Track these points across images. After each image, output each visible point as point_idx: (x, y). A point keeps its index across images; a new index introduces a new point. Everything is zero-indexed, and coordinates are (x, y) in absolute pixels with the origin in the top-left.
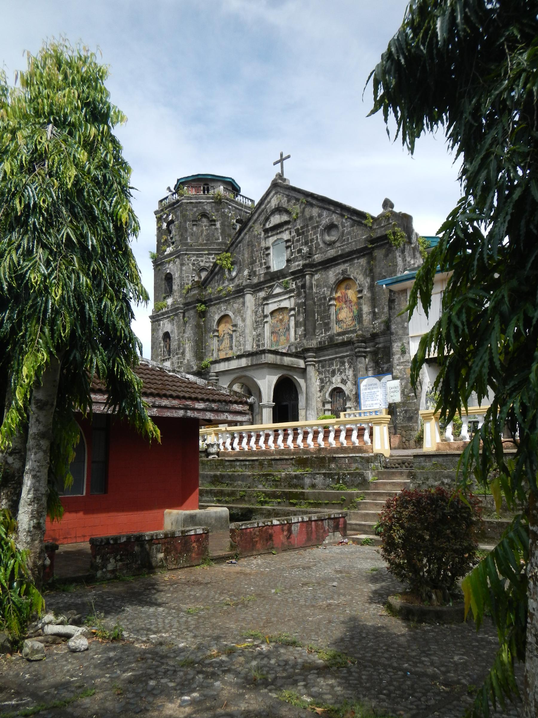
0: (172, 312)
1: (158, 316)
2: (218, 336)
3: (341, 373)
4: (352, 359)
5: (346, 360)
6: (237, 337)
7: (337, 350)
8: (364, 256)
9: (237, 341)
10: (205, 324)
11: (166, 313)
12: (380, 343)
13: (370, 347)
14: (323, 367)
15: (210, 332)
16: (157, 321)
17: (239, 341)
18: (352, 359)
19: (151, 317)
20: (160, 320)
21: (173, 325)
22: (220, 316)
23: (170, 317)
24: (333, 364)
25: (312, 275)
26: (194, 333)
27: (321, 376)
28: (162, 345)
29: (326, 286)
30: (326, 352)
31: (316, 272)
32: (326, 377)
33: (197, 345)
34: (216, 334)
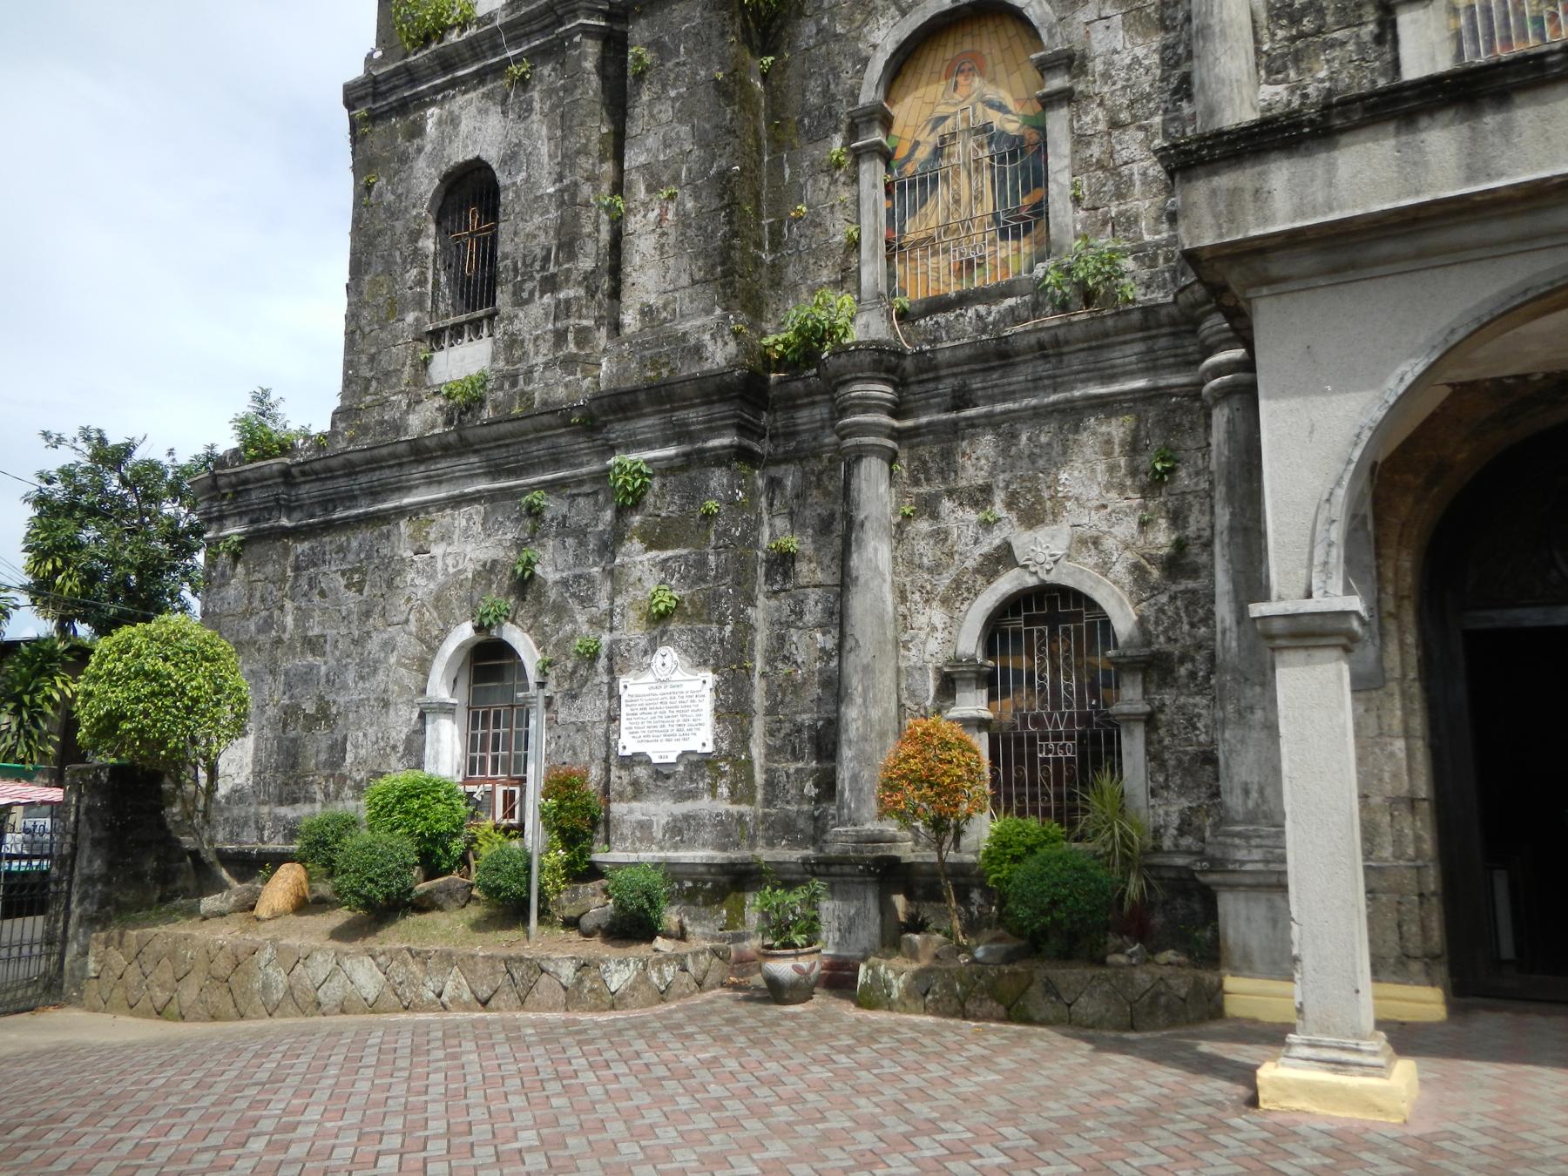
0: (514, 41)
1: (411, 75)
2: (887, 157)
6: (1080, 140)
9: (1081, 166)
10: (773, 93)
11: (474, 48)
15: (818, 135)
16: (402, 108)
17: (1106, 166)
19: (353, 96)
20: (421, 102)
21: (526, 112)
22: (916, 20)
23: (499, 70)
26: (701, 140)
28: (429, 244)
33: (731, 207)
34: (878, 136)
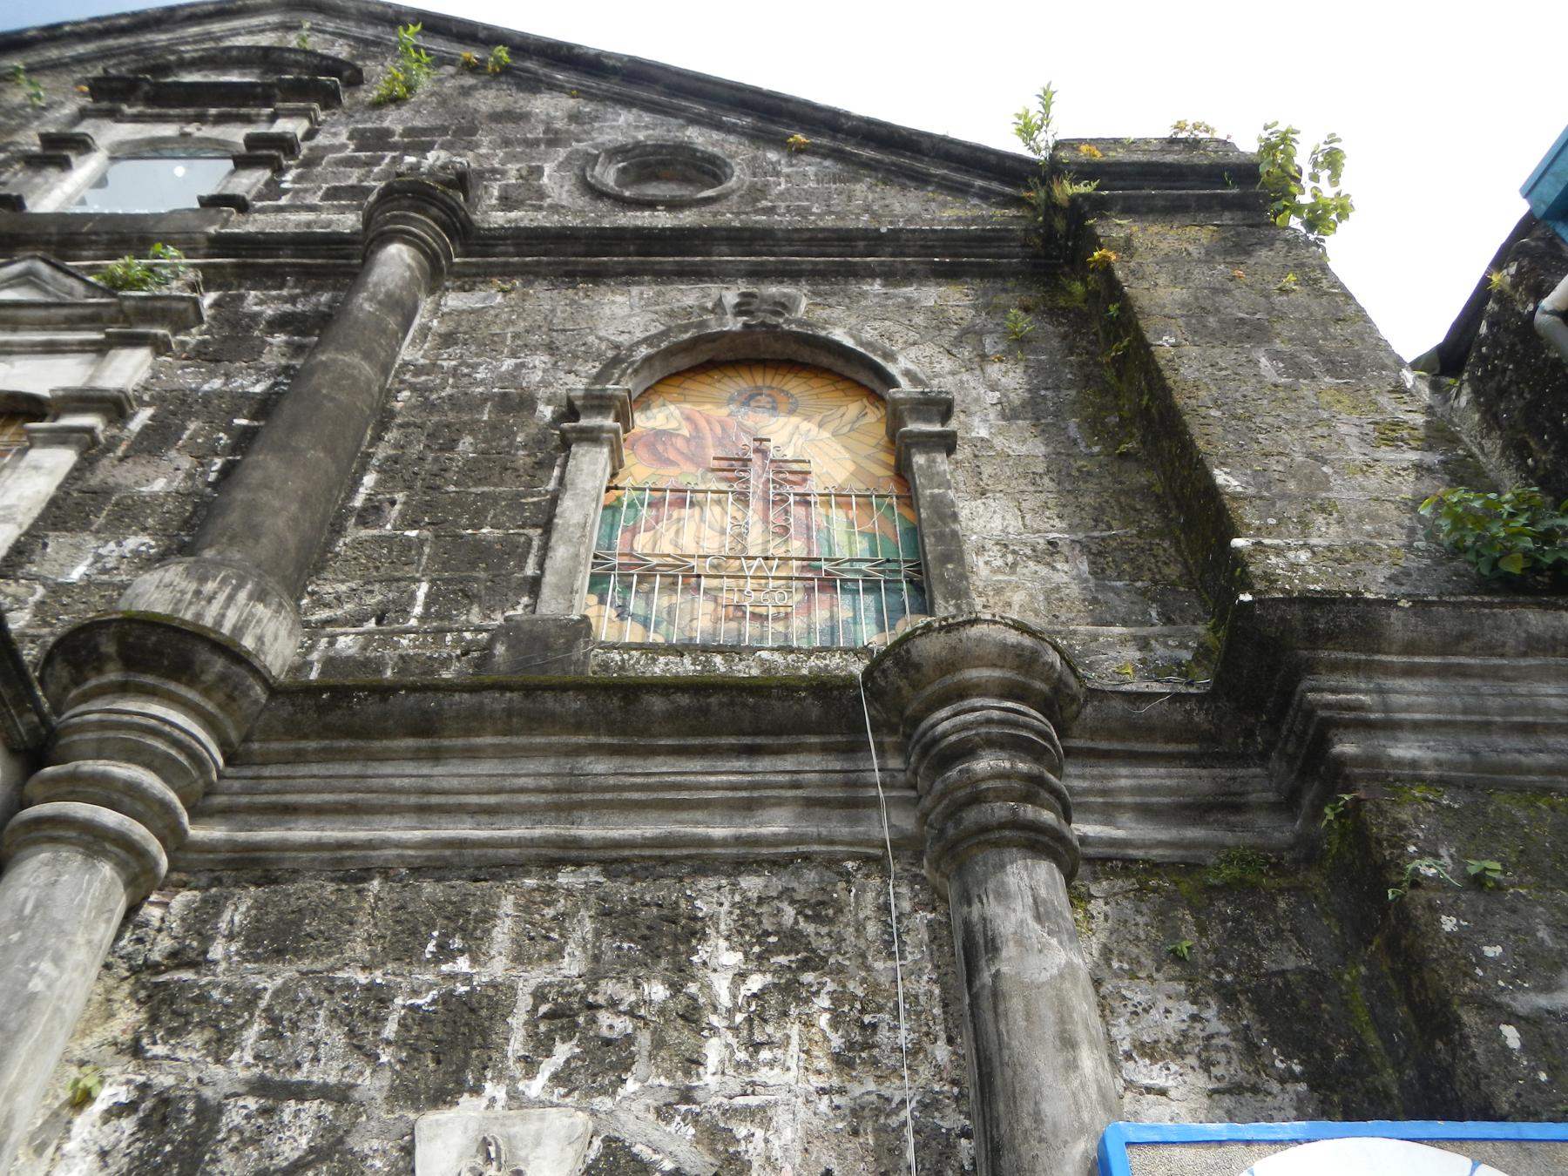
3: (606, 1063)
4: (819, 909)
5: (713, 900)
7: (599, 766)
8: (948, 274)
12: (1391, 727)
13: (1108, 812)
14: (272, 940)
18: (819, 909)
24: (469, 928)
25: (436, 274)
27: (184, 1064)
29: (551, 349)
30: (404, 774)
31: (469, 279)
32: (274, 1091)
